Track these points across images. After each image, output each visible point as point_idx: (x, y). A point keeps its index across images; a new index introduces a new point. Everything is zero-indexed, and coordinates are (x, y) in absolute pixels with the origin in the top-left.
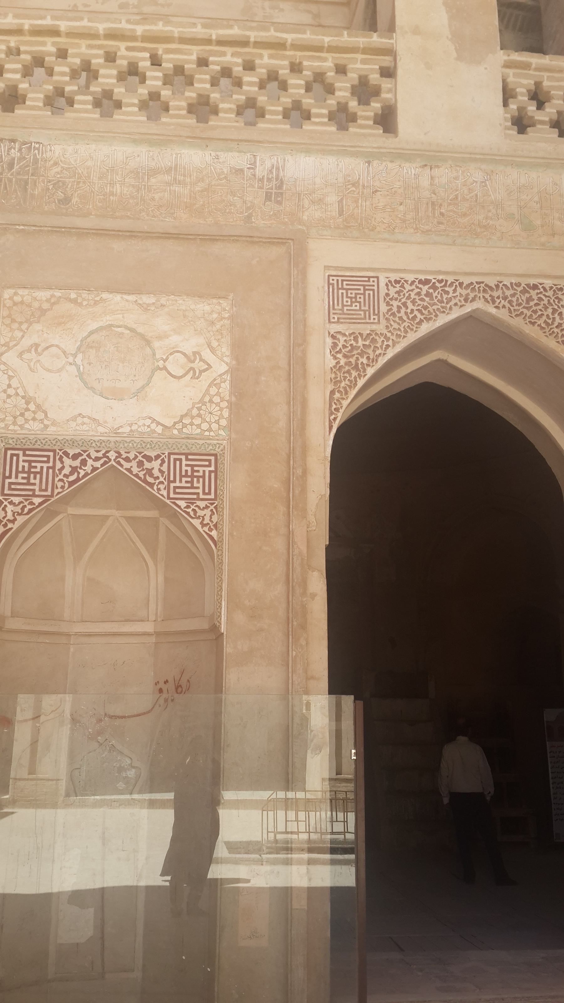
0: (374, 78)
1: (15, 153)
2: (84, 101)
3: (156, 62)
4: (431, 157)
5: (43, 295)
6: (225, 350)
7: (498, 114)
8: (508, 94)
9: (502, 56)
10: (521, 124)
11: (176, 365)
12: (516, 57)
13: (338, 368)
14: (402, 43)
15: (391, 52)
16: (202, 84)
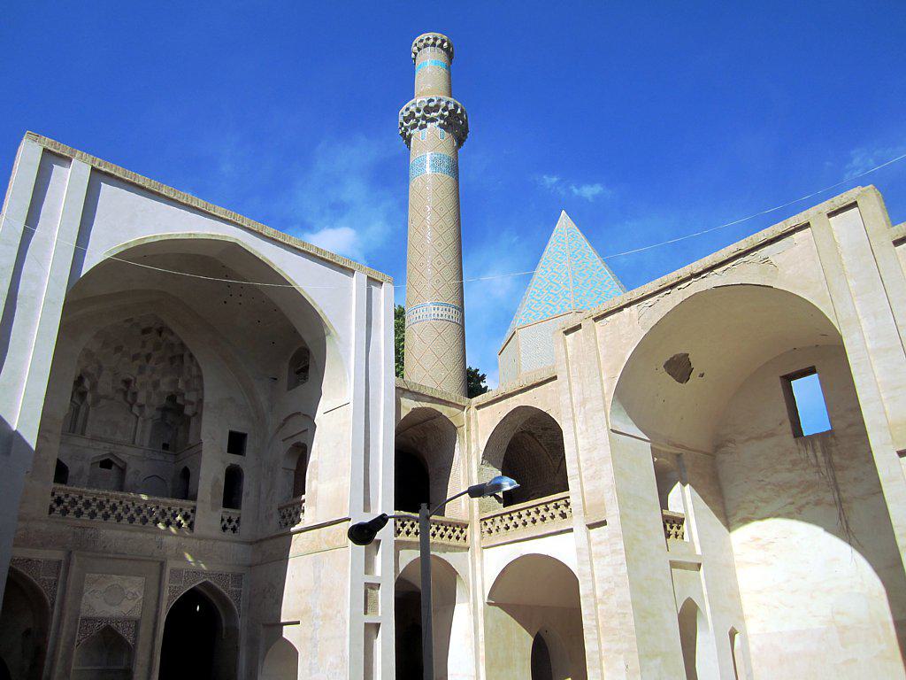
0: (189, 513)
1: (92, 532)
2: (113, 517)
3: (133, 504)
4: (200, 539)
5: (96, 575)
6: (142, 592)
7: (219, 526)
8: (223, 520)
9: (222, 509)
10: (224, 528)
11: (130, 596)
12: (226, 510)
13: (170, 596)
14: (199, 505)
15: (195, 507)
16: (145, 513)
